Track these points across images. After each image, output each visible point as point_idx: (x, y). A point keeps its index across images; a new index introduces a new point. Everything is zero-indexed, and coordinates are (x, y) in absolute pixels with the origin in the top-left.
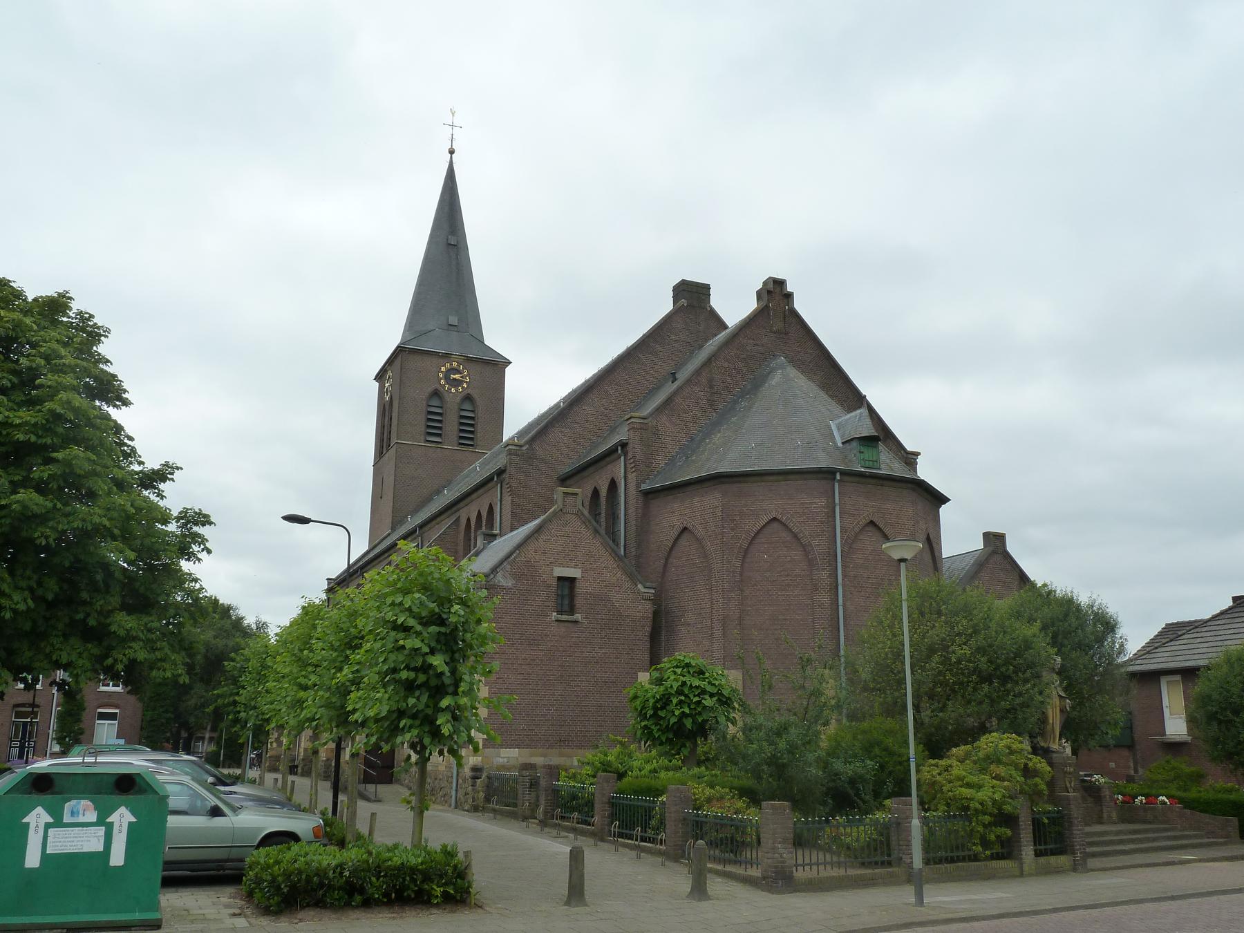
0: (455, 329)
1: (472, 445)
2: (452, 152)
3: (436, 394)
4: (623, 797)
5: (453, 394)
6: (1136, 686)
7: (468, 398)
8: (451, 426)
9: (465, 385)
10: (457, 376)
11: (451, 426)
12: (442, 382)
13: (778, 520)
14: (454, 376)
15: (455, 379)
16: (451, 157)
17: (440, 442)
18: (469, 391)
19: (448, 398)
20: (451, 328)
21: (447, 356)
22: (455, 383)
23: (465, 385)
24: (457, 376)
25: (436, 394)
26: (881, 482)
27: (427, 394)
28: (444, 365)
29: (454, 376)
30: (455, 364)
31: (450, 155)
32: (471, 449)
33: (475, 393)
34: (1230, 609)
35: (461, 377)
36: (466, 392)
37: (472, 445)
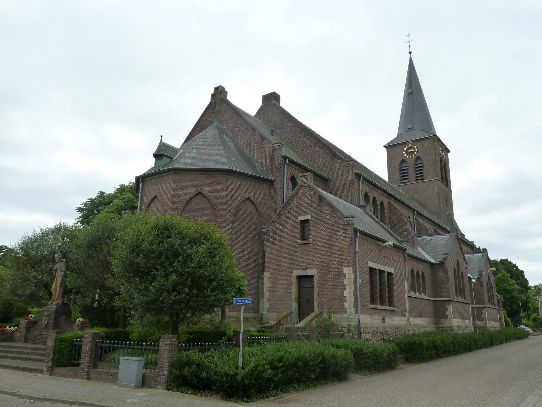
0: (412, 129)
1: (423, 179)
2: (410, 53)
3: (403, 161)
4: (330, 333)
5: (410, 159)
6: (405, 341)
7: (418, 158)
8: (412, 173)
9: (416, 153)
10: (411, 150)
11: (412, 173)
12: (405, 155)
13: (202, 194)
14: (410, 151)
15: (410, 152)
16: (410, 55)
17: (408, 182)
18: (418, 155)
19: (408, 161)
20: (410, 129)
21: (405, 143)
22: (412, 154)
23: (416, 153)
24: (411, 150)
25: (403, 161)
26: (160, 175)
27: (399, 163)
28: (405, 148)
29: (410, 151)
30: (410, 146)
31: (410, 54)
32: (422, 181)
33: (421, 156)
34: (489, 259)
35: (414, 150)
36: (417, 156)
37: (423, 179)
